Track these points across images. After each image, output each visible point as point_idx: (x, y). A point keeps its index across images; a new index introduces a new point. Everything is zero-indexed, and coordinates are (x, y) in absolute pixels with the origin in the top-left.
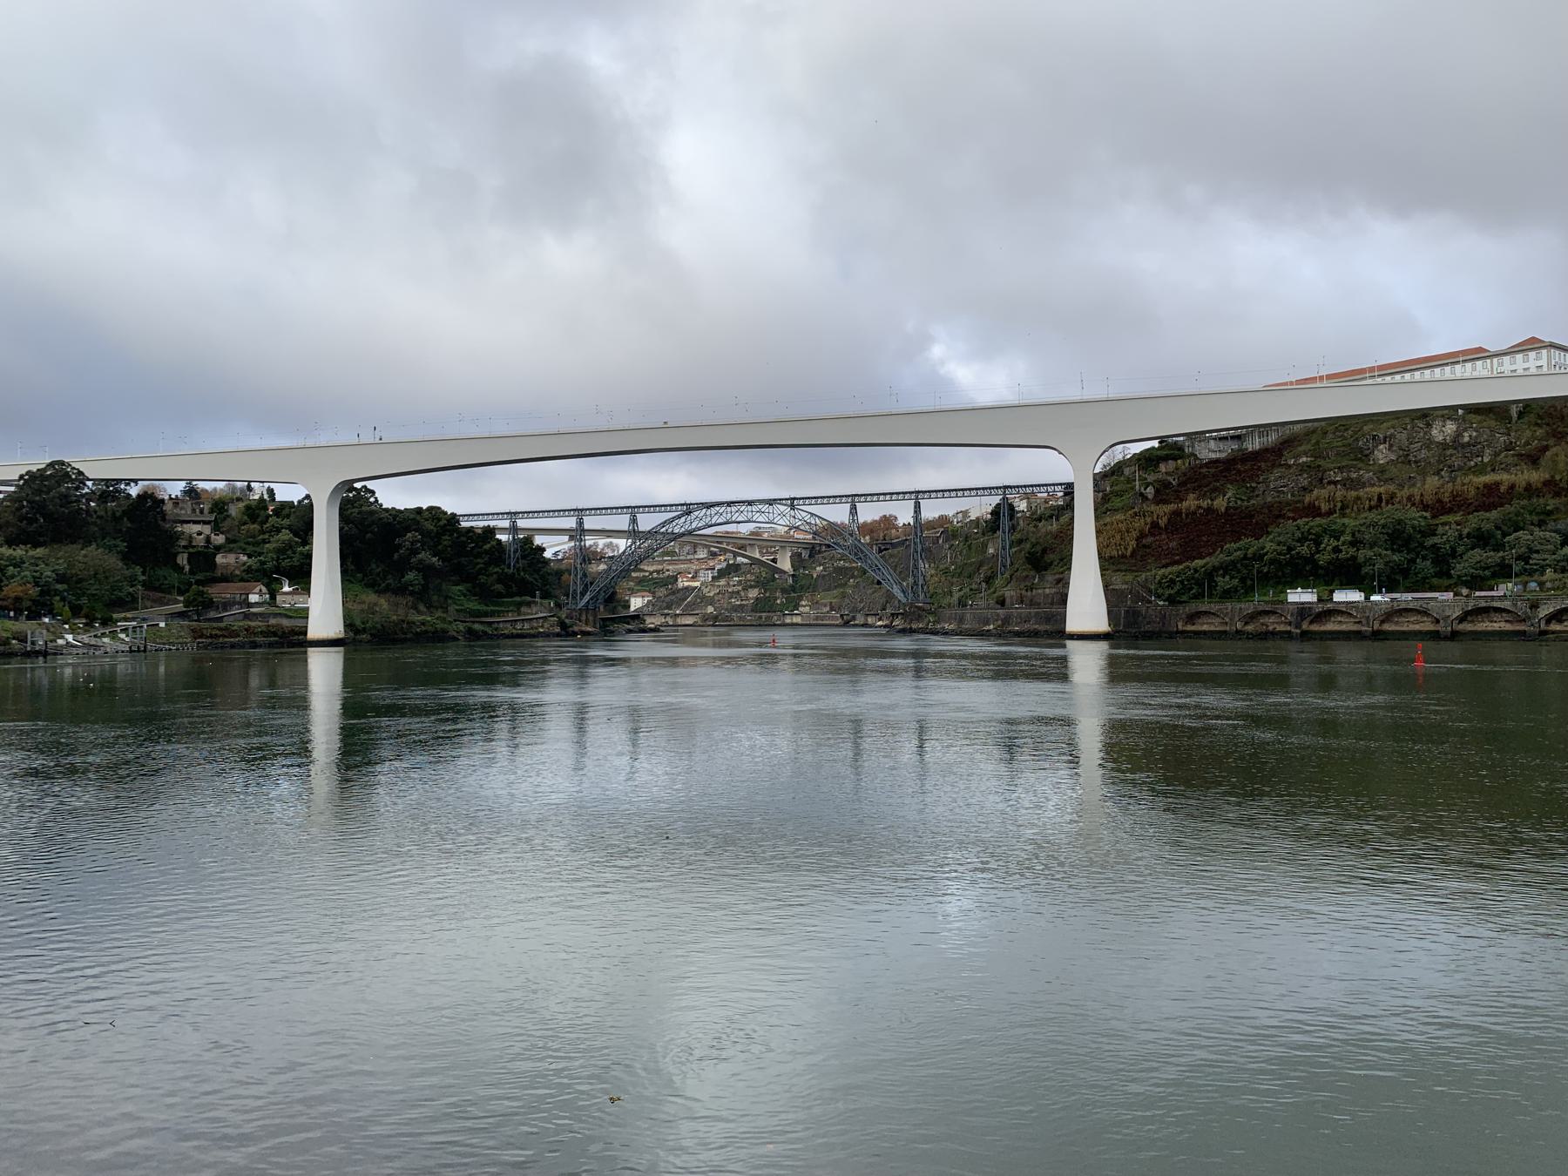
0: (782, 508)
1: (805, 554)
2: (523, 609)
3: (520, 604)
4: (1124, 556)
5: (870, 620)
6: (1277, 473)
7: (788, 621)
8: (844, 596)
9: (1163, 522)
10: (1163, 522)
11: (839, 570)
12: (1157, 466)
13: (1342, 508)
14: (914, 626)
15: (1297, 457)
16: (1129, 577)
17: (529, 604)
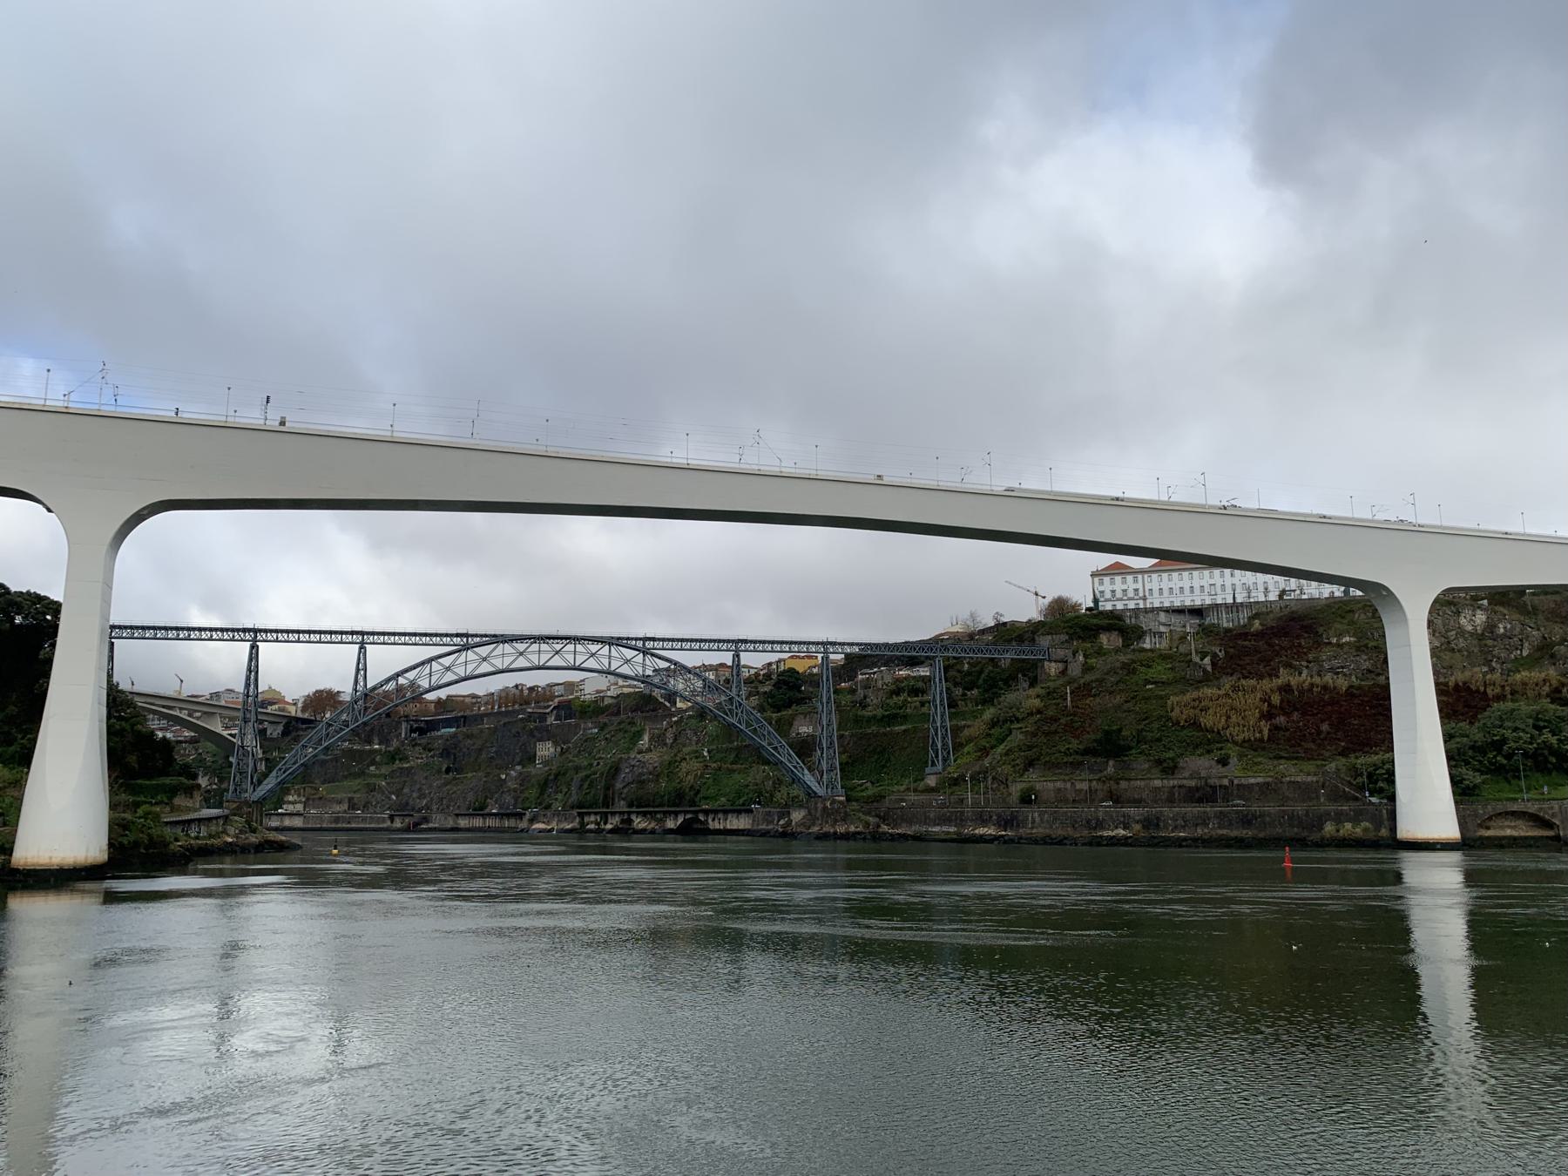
0: (629, 654)
1: (274, 731)
2: (179, 801)
3: (173, 791)
4: (1261, 740)
5: (463, 823)
6: (1326, 653)
7: (274, 823)
8: (372, 789)
9: (1276, 699)
10: (1276, 699)
11: (350, 754)
12: (1096, 636)
13: (1513, 693)
14: (841, 829)
15: (1340, 635)
16: (1310, 766)
17: (189, 791)
